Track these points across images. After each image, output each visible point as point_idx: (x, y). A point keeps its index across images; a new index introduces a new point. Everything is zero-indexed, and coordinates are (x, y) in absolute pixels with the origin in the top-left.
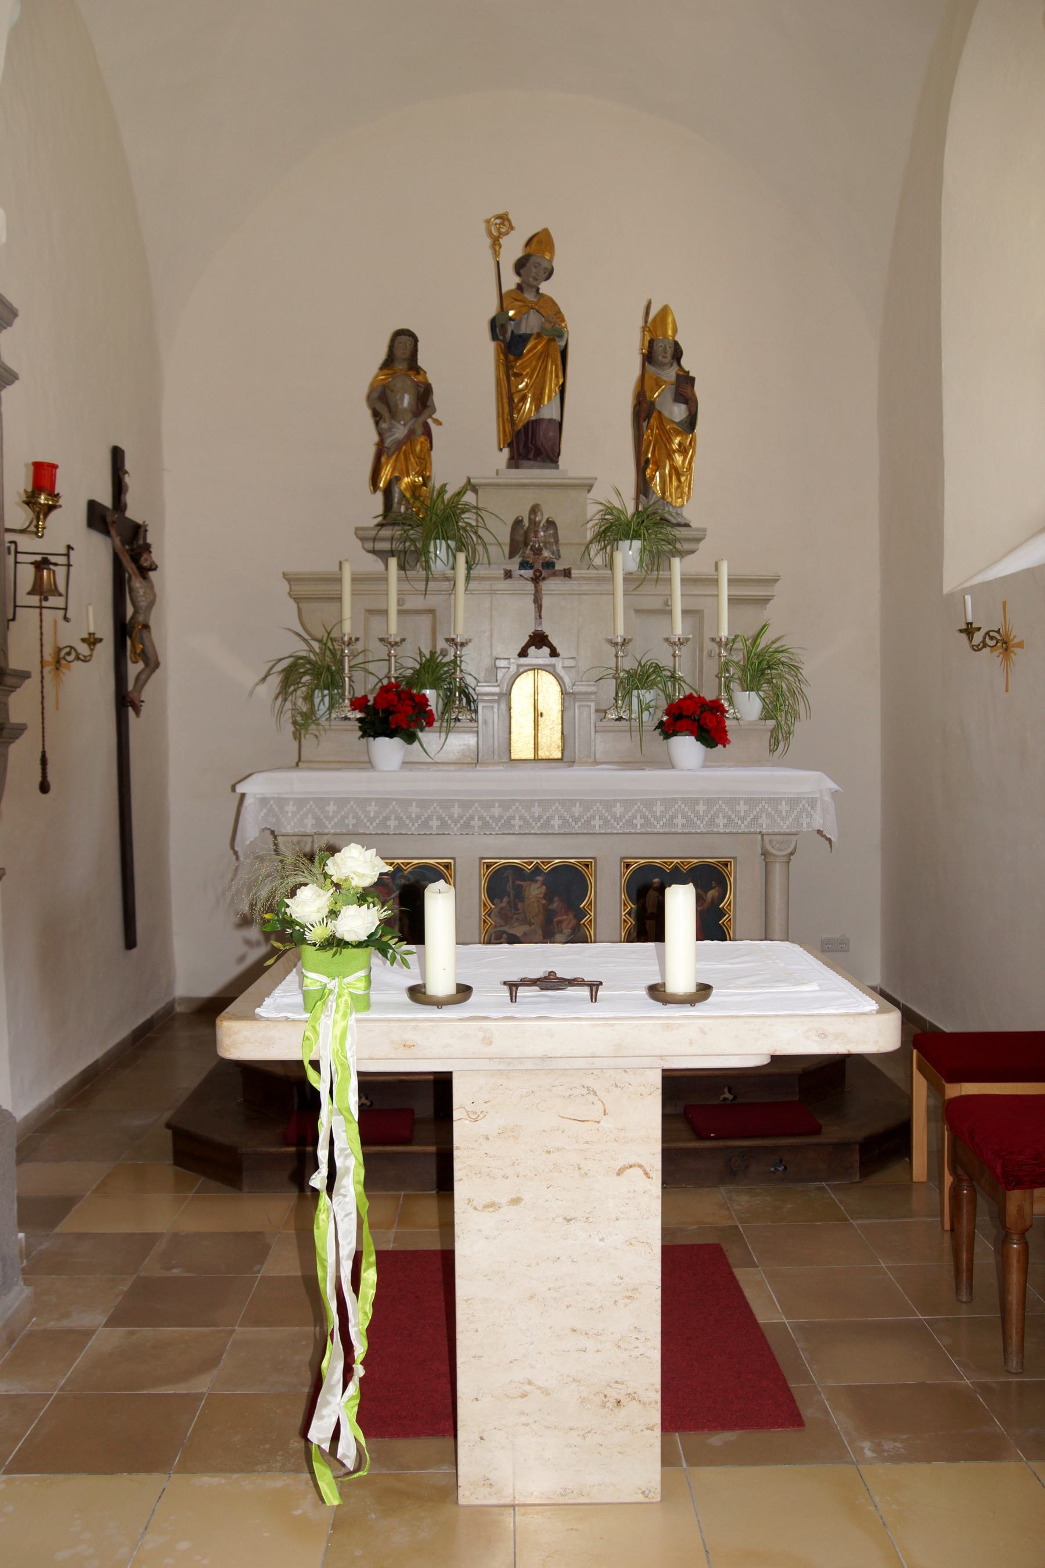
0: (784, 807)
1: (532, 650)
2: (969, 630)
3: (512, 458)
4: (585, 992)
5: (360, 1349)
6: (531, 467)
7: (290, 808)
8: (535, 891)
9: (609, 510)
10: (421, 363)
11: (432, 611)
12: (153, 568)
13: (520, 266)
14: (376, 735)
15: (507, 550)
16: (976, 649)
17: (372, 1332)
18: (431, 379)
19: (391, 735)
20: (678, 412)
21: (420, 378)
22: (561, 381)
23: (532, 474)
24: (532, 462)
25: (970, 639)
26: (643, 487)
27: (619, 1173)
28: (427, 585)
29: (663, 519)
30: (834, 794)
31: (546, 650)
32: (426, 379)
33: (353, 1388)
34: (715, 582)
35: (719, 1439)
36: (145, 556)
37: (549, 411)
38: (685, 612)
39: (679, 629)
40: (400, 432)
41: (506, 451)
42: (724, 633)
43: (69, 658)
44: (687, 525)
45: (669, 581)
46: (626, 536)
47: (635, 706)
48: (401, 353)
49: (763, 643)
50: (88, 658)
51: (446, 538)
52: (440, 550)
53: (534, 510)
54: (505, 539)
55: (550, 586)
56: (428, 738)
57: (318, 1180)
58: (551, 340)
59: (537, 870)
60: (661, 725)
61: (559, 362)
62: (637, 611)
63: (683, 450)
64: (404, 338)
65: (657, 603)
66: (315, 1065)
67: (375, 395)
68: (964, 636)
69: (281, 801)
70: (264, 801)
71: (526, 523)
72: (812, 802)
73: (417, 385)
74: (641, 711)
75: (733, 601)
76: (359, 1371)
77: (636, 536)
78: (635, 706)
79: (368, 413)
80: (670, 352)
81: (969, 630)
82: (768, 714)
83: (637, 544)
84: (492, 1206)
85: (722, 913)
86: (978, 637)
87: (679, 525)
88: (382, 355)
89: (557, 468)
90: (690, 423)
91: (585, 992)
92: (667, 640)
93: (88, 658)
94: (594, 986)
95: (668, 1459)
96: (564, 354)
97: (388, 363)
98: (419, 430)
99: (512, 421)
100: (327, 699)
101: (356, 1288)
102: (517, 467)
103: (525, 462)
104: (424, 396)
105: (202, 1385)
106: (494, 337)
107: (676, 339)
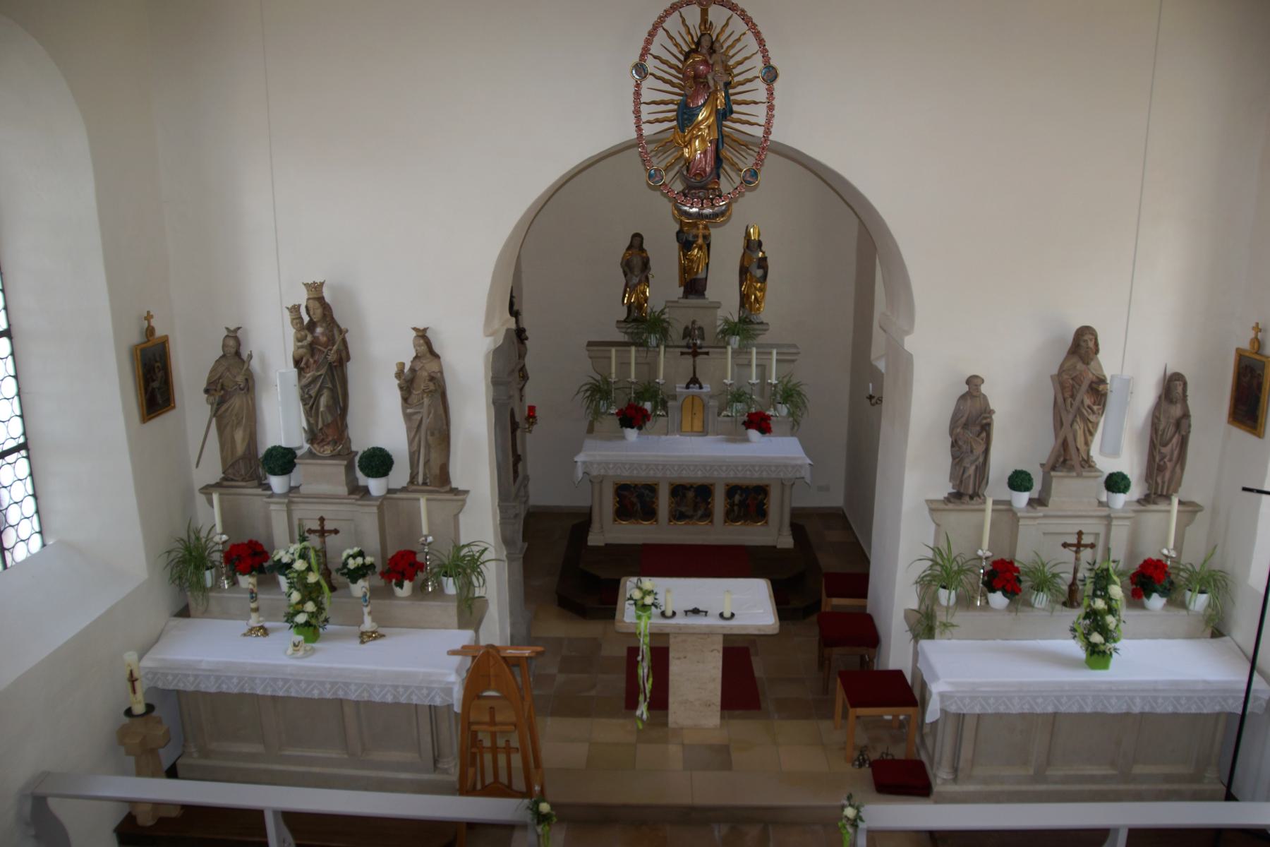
1: (691, 386)
3: (684, 292)
4: (704, 614)
5: (648, 695)
6: (692, 299)
7: (595, 466)
8: (691, 494)
9: (726, 321)
10: (645, 246)
11: (648, 364)
12: (527, 339)
14: (627, 427)
15: (682, 335)
16: (873, 405)
17: (651, 692)
18: (650, 254)
20: (759, 273)
21: (644, 255)
22: (707, 261)
23: (693, 301)
24: (693, 296)
25: (871, 401)
27: (712, 651)
28: (647, 353)
29: (750, 321)
31: (697, 385)
32: (647, 254)
33: (646, 703)
35: (737, 712)
36: (523, 335)
38: (757, 365)
40: (635, 280)
41: (682, 289)
46: (733, 334)
47: (734, 410)
48: (637, 240)
51: (655, 333)
52: (653, 340)
53: (694, 322)
54: (681, 332)
55: (699, 359)
56: (648, 425)
57: (640, 658)
59: (692, 487)
60: (744, 423)
61: (706, 253)
62: (737, 365)
63: (761, 290)
64: (638, 239)
65: (746, 362)
66: (640, 634)
67: (624, 263)
68: (868, 401)
69: (592, 463)
70: (584, 463)
71: (690, 328)
72: (801, 466)
73: (643, 258)
74: (736, 414)
75: (777, 360)
76: (648, 700)
77: (738, 334)
78: (734, 410)
79: (621, 270)
80: (756, 245)
82: (791, 414)
83: (738, 338)
84: (679, 658)
85: (764, 504)
87: (758, 323)
88: (627, 243)
90: (764, 278)
91: (704, 614)
94: (706, 612)
95: (722, 717)
97: (629, 248)
98: (643, 279)
100: (605, 405)
101: (647, 680)
102: (687, 298)
103: (691, 296)
104: (645, 265)
105: (593, 693)
106: (678, 241)
107: (760, 239)
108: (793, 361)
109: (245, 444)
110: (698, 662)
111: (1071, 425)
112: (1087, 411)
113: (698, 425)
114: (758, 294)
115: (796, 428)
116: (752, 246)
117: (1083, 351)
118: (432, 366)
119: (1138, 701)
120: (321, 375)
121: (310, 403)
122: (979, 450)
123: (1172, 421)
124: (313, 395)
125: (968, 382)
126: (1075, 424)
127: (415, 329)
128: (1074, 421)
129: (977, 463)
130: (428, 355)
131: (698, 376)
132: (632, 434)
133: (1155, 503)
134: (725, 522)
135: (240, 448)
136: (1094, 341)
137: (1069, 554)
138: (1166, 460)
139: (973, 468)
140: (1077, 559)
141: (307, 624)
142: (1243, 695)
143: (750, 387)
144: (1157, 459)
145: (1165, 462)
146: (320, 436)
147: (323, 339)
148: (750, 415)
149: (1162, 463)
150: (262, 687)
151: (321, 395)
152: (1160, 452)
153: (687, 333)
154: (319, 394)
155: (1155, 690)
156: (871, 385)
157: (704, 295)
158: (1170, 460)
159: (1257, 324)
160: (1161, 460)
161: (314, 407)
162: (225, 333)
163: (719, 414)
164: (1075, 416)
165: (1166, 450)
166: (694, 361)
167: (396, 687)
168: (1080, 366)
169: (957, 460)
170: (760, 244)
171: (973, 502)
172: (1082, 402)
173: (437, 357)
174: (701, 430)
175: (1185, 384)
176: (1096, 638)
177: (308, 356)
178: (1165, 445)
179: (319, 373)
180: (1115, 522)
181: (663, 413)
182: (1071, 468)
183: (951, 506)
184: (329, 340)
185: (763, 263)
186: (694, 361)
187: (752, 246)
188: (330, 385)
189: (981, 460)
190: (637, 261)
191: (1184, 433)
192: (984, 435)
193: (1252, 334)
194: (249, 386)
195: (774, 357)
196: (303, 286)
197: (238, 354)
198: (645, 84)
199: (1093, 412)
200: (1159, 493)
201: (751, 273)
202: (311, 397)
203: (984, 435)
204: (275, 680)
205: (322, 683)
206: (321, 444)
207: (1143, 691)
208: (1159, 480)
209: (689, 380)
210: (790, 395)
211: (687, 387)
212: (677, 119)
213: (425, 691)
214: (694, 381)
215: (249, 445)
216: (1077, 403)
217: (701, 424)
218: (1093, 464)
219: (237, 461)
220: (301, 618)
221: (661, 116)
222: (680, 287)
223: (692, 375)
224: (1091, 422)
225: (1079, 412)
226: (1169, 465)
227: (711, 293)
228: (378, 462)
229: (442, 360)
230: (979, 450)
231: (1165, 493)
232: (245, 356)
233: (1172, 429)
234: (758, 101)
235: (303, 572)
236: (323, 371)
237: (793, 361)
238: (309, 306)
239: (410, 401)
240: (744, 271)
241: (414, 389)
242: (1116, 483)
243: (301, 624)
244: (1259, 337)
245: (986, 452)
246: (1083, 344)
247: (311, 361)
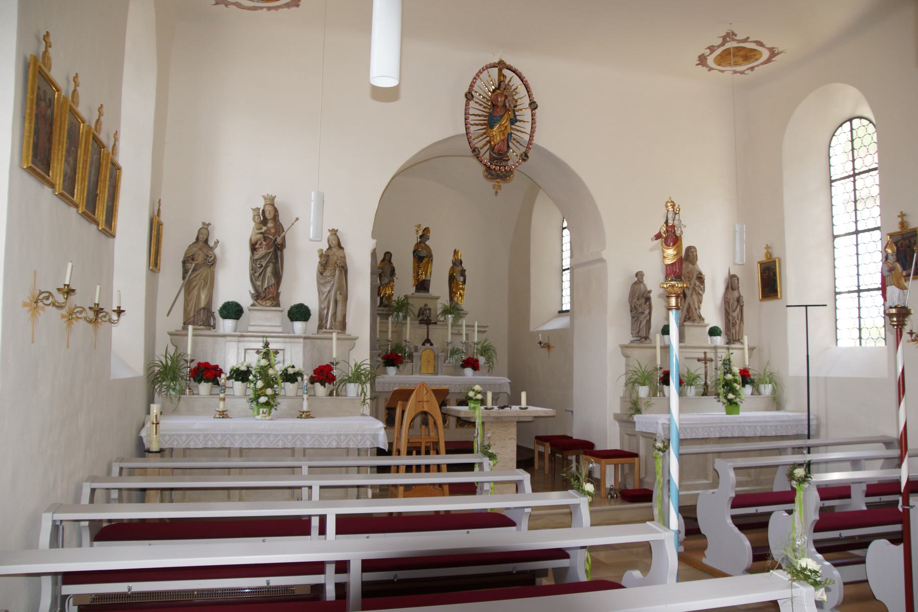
0: (497, 386)
2: (540, 343)
10: (392, 261)
13: (421, 237)
16: (542, 347)
19: (394, 366)
20: (462, 279)
26: (451, 299)
27: (510, 439)
30: (510, 383)
34: (473, 326)
37: (428, 278)
39: (464, 339)
41: (415, 287)
42: (476, 340)
43: (103, 319)
44: (463, 310)
45: (461, 326)
49: (485, 344)
50: (116, 322)
53: (426, 305)
57: (476, 435)
58: (429, 258)
60: (462, 365)
68: (539, 345)
75: (478, 332)
81: (540, 343)
86: (542, 345)
89: (429, 293)
90: (464, 282)
92: (461, 342)
93: (116, 322)
96: (432, 260)
99: (418, 280)
104: (393, 272)
108: (485, 332)
109: (207, 301)
110: (502, 447)
111: (691, 296)
113: (431, 370)
114: (461, 291)
115: (490, 371)
116: (457, 263)
117: (691, 258)
118: (339, 253)
119: (758, 428)
120: (270, 252)
121: (256, 273)
122: (647, 312)
123: (736, 299)
124: (264, 265)
125: (637, 275)
127: (329, 230)
129: (646, 319)
130: (337, 247)
131: (430, 338)
132: (392, 370)
133: (733, 344)
134: (457, 427)
135: (203, 304)
137: (702, 364)
138: (736, 319)
139: (645, 321)
140: (706, 367)
141: (267, 404)
142: (806, 423)
143: (462, 344)
145: (735, 322)
146: (263, 295)
147: (273, 231)
148: (464, 361)
149: (734, 322)
150: (239, 442)
151: (268, 266)
153: (421, 312)
154: (267, 266)
155: (766, 422)
156: (540, 335)
157: (429, 291)
158: (738, 319)
159: (767, 245)
160: (733, 320)
161: (263, 274)
162: (201, 226)
163: (445, 362)
164: (692, 292)
166: (428, 328)
167: (339, 435)
168: (690, 265)
169: (636, 318)
170: (461, 263)
171: (646, 342)
172: (695, 284)
173: (342, 248)
174: (433, 372)
175: (738, 280)
176: (731, 396)
177: (262, 240)
178: (734, 312)
179: (269, 251)
181: (409, 361)
182: (694, 321)
183: (635, 345)
184: (276, 231)
185: (463, 273)
186: (428, 328)
187: (457, 263)
188: (274, 261)
193: (765, 251)
194: (211, 263)
195: (476, 329)
196: (262, 197)
197: (206, 241)
198: (472, 103)
200: (734, 339)
201: (457, 280)
202: (262, 266)
203: (648, 303)
204: (250, 435)
205: (285, 436)
206: (264, 300)
207: (760, 422)
208: (734, 332)
209: (424, 340)
210: (485, 350)
211: (423, 344)
212: (488, 120)
213: (359, 438)
214: (428, 341)
215: (208, 303)
217: (433, 368)
219: (200, 310)
220: (263, 400)
221: (477, 122)
222: (413, 286)
223: (426, 338)
225: (694, 289)
227: (433, 291)
228: (300, 313)
229: (345, 251)
230: (647, 312)
231: (737, 339)
232: (211, 243)
233: (736, 303)
234: (525, 120)
235: (265, 367)
236: (272, 250)
237: (485, 332)
238: (265, 210)
239: (324, 274)
240: (452, 278)
241: (328, 267)
242: (714, 332)
243: (263, 403)
244: (769, 251)
245: (650, 313)
246: (690, 254)
247: (264, 243)
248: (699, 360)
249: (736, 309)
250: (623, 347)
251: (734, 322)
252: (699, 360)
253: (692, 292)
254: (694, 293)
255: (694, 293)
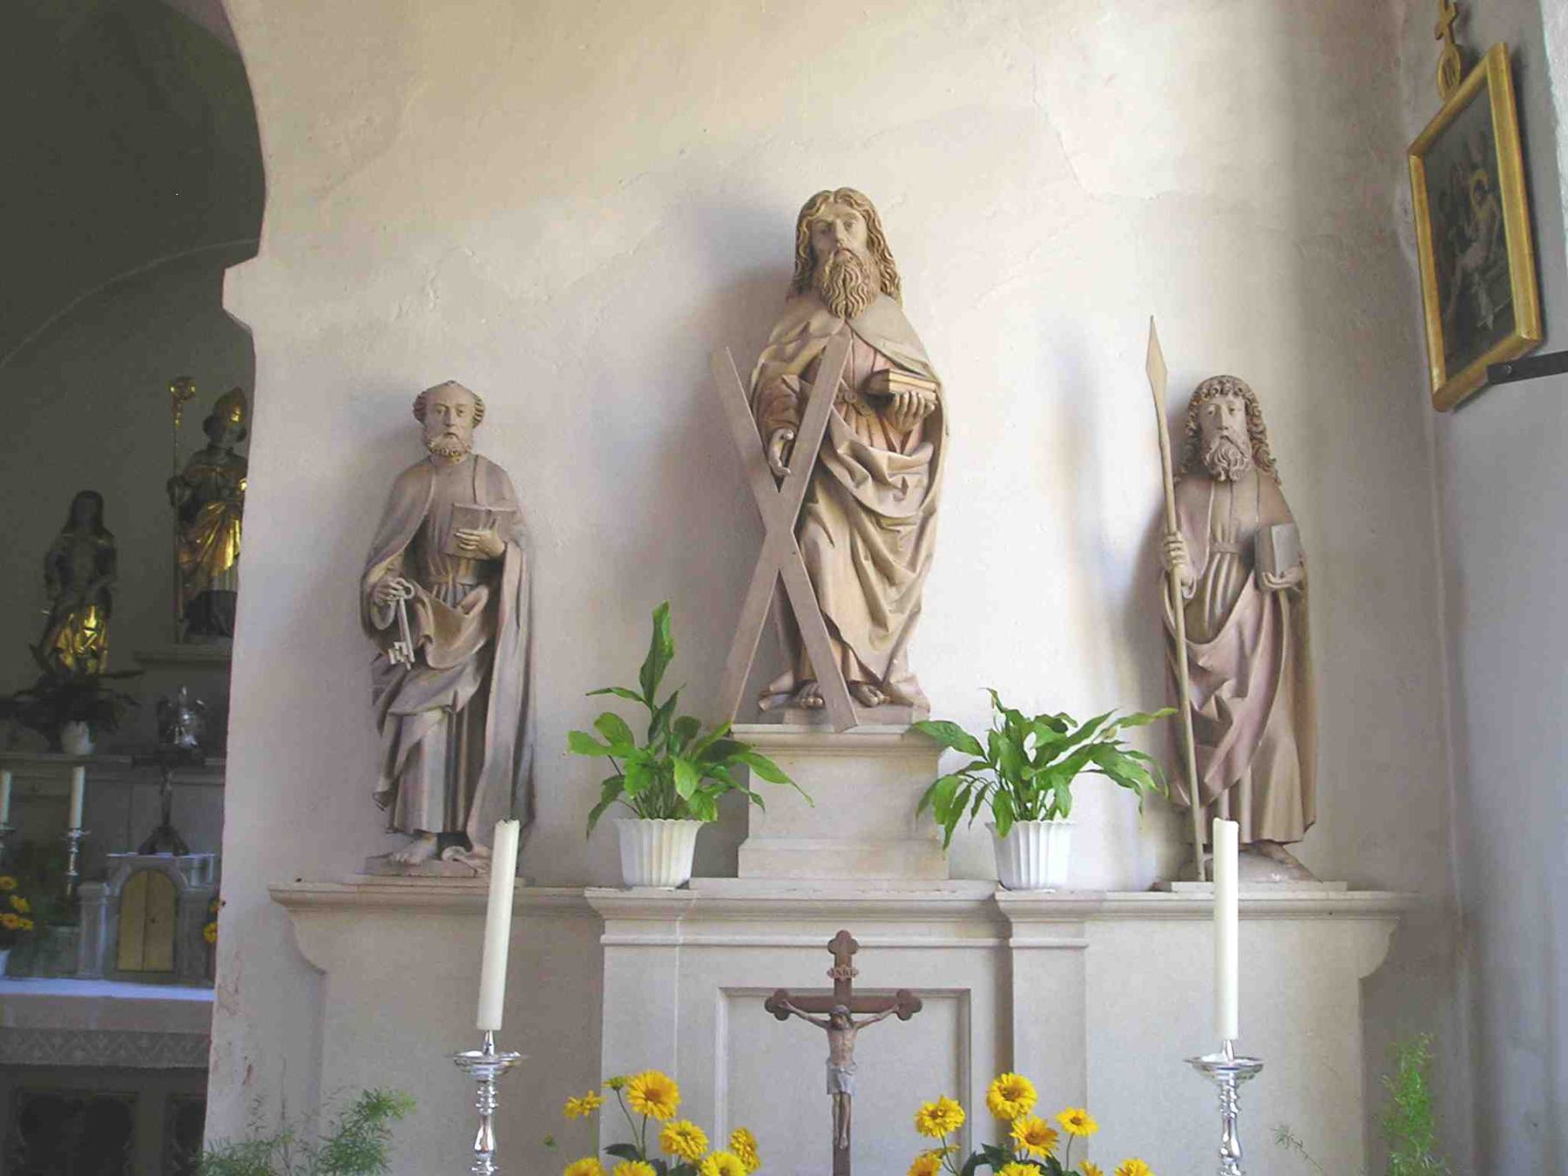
10: (107, 525)
97: (73, 524)
111: (800, 529)
112: (852, 473)
123: (1231, 547)
125: (422, 406)
126: (812, 528)
128: (806, 514)
136: (860, 228)
138: (1226, 692)
144: (1191, 693)
145: (1220, 704)
149: (1211, 709)
152: (1197, 672)
158: (1241, 691)
164: (810, 497)
165: (1220, 653)
168: (818, 321)
172: (828, 440)
174: (168, 966)
180: (1022, 935)
189: (466, 690)
190: (82, 564)
191: (1275, 581)
192: (483, 593)
199: (879, 480)
208: (1213, 777)
216: (808, 447)
218: (905, 689)
224: (876, 517)
226: (1243, 712)
233: (1229, 572)
248: (780, 1004)
249: (1228, 610)
250: (294, 904)
251: (1211, 709)
252: (780, 1004)
253: (810, 497)
254: (823, 507)
255: (823, 507)
